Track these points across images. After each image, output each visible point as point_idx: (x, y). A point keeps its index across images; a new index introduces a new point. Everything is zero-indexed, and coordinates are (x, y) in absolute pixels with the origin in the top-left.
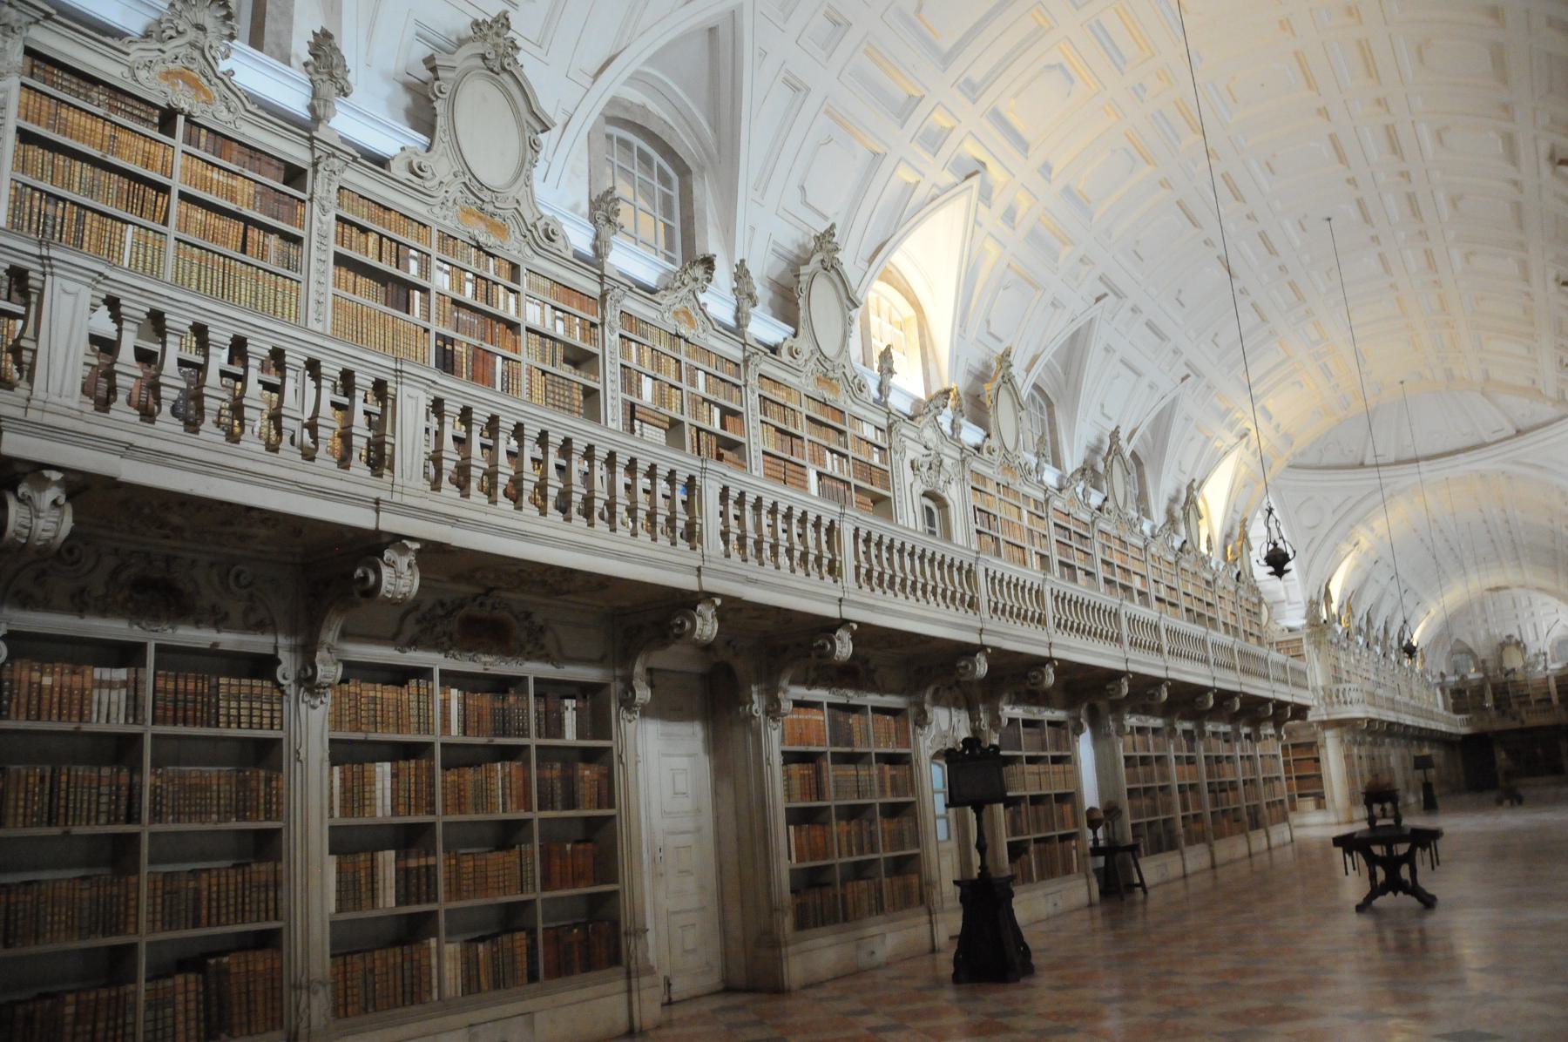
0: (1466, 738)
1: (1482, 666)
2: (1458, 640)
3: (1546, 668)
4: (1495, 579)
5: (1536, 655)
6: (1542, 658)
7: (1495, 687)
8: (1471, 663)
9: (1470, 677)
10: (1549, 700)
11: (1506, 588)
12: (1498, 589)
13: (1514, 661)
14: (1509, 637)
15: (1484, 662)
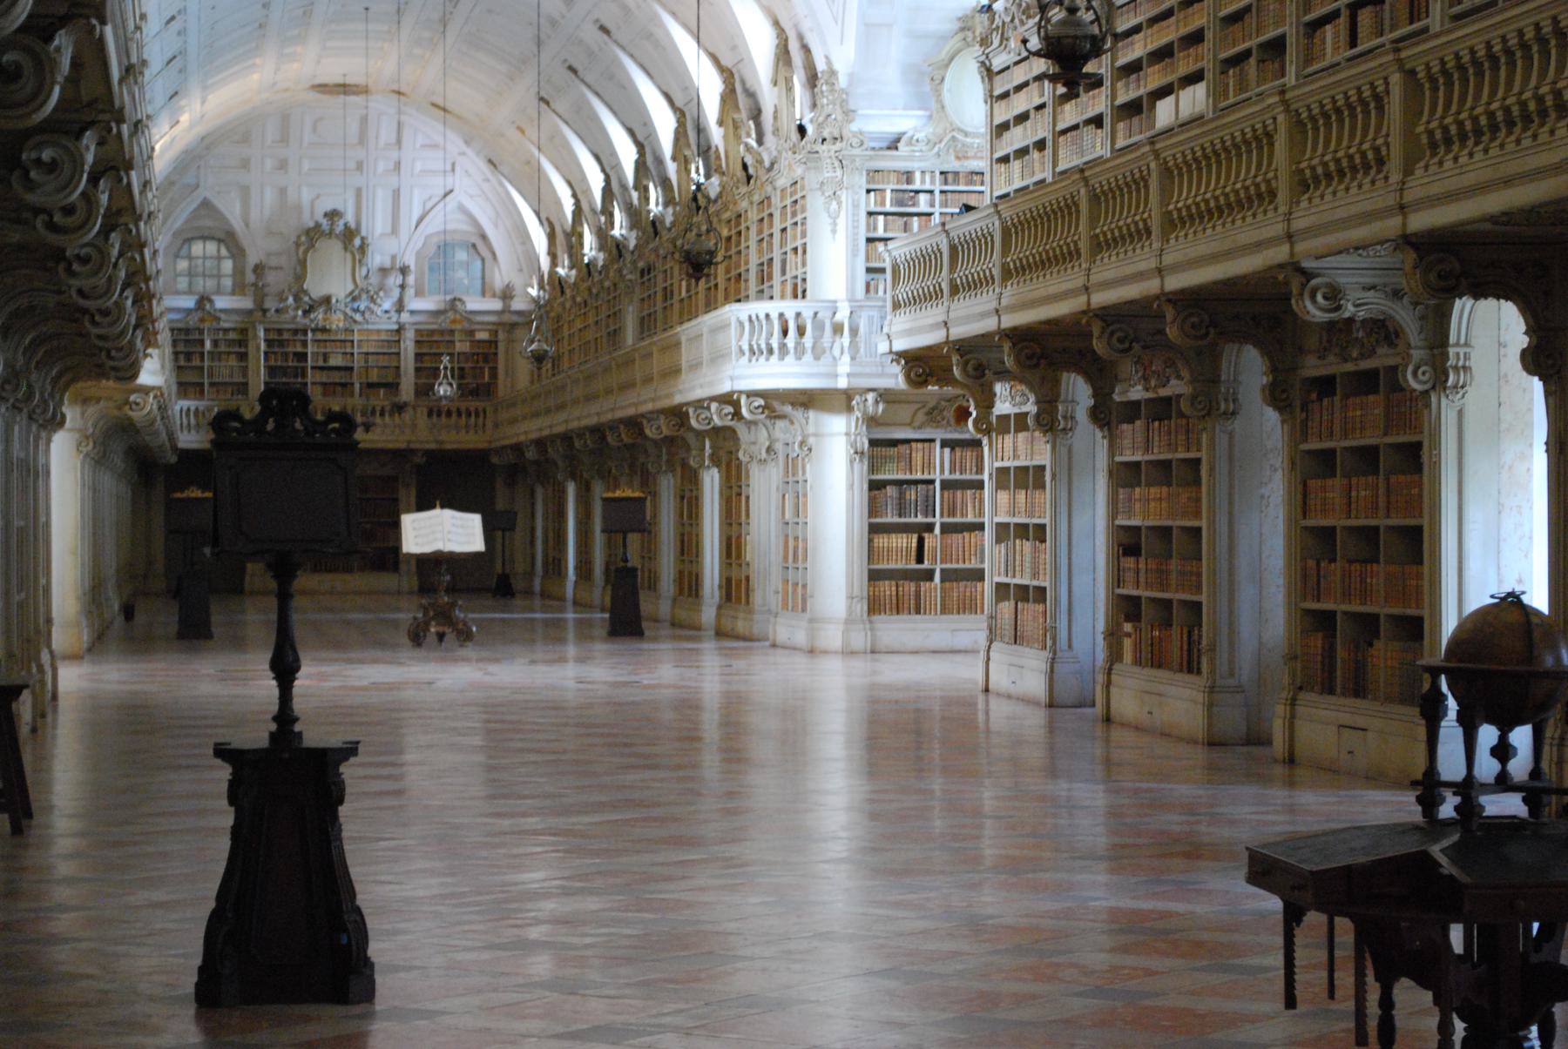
0: (187, 455)
1: (252, 280)
2: (206, 204)
3: (400, 307)
4: (336, 69)
5: (384, 271)
6: (394, 280)
7: (276, 341)
8: (228, 266)
9: (222, 303)
10: (393, 387)
11: (363, 90)
12: (344, 89)
13: (331, 278)
14: (333, 215)
15: (259, 269)
